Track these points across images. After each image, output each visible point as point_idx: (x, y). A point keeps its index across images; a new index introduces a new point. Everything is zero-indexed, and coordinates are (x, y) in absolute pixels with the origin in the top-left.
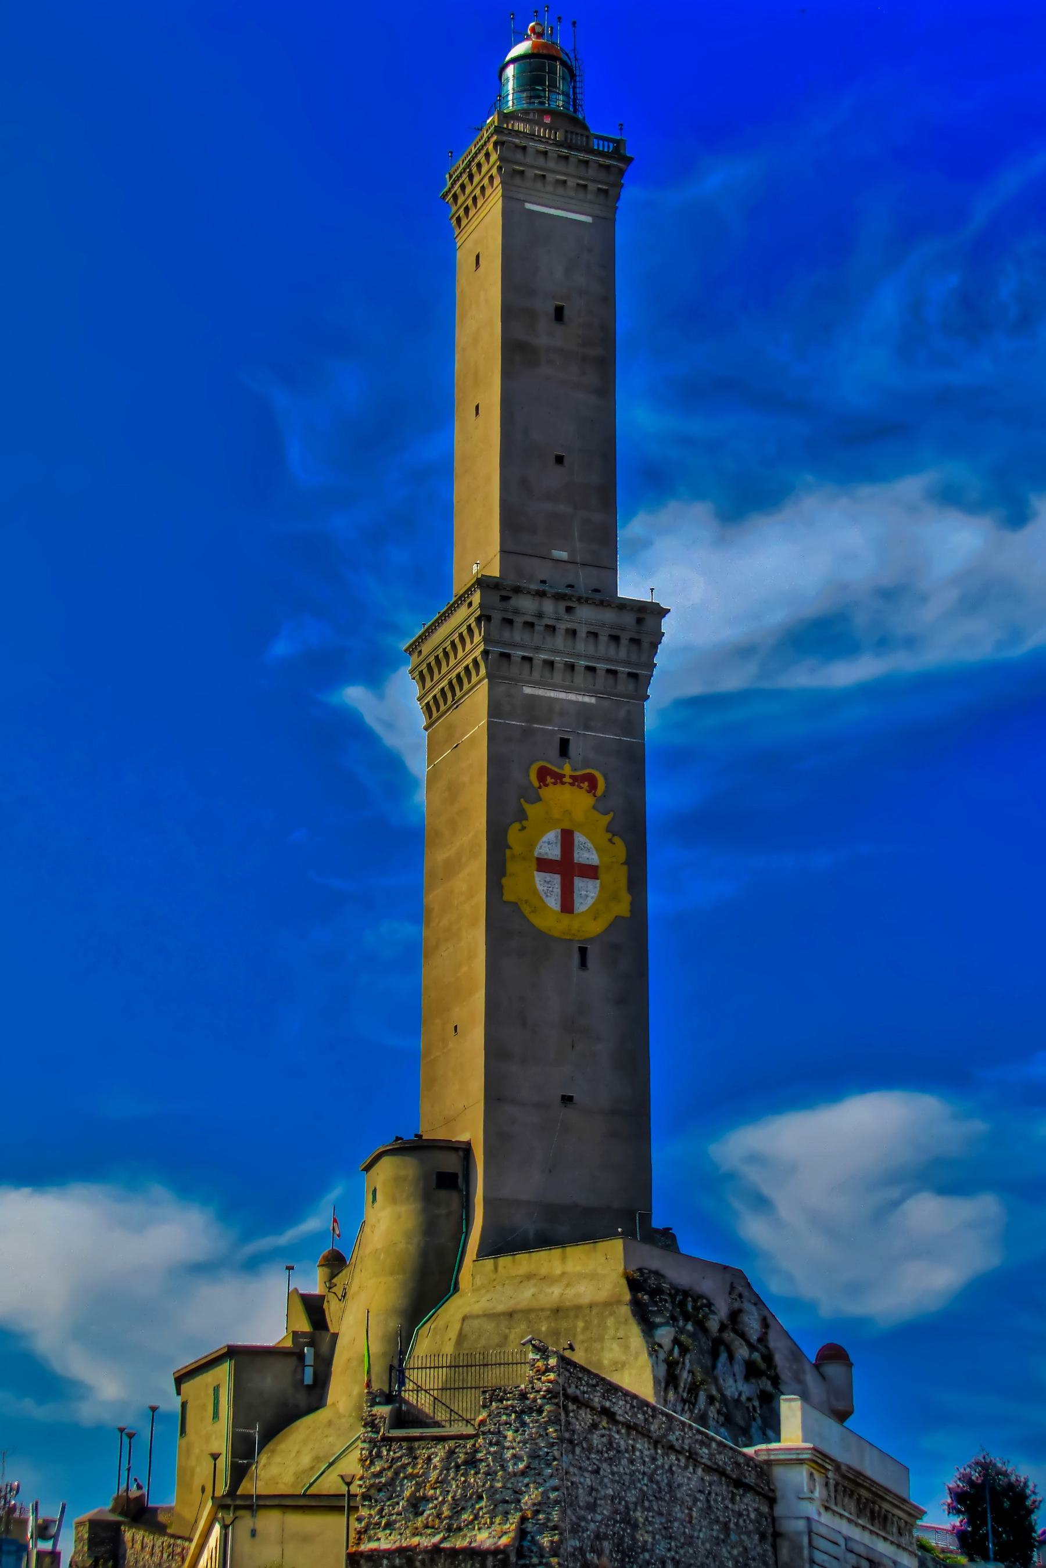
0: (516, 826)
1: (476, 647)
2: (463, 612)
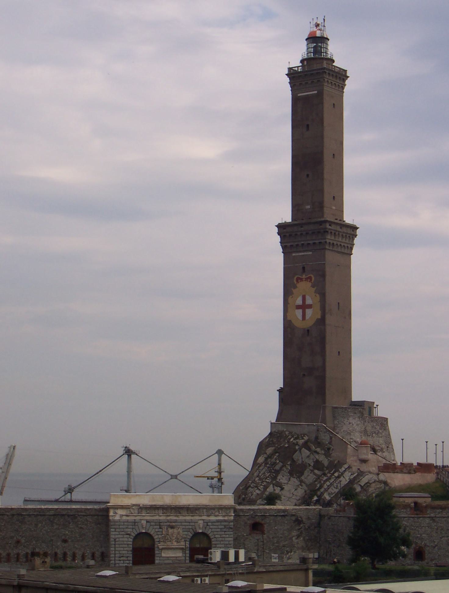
0: (291, 296)
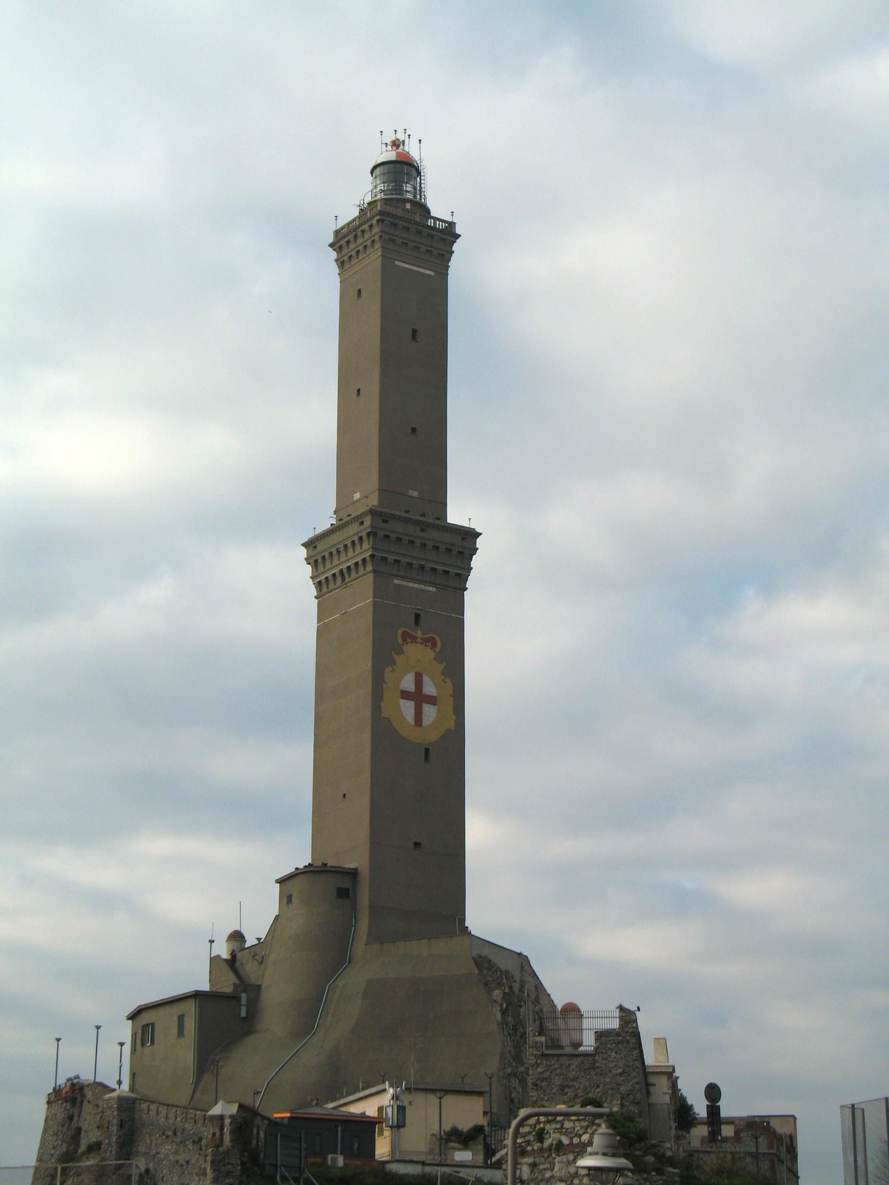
0: (389, 669)
1: (365, 550)
2: (354, 529)
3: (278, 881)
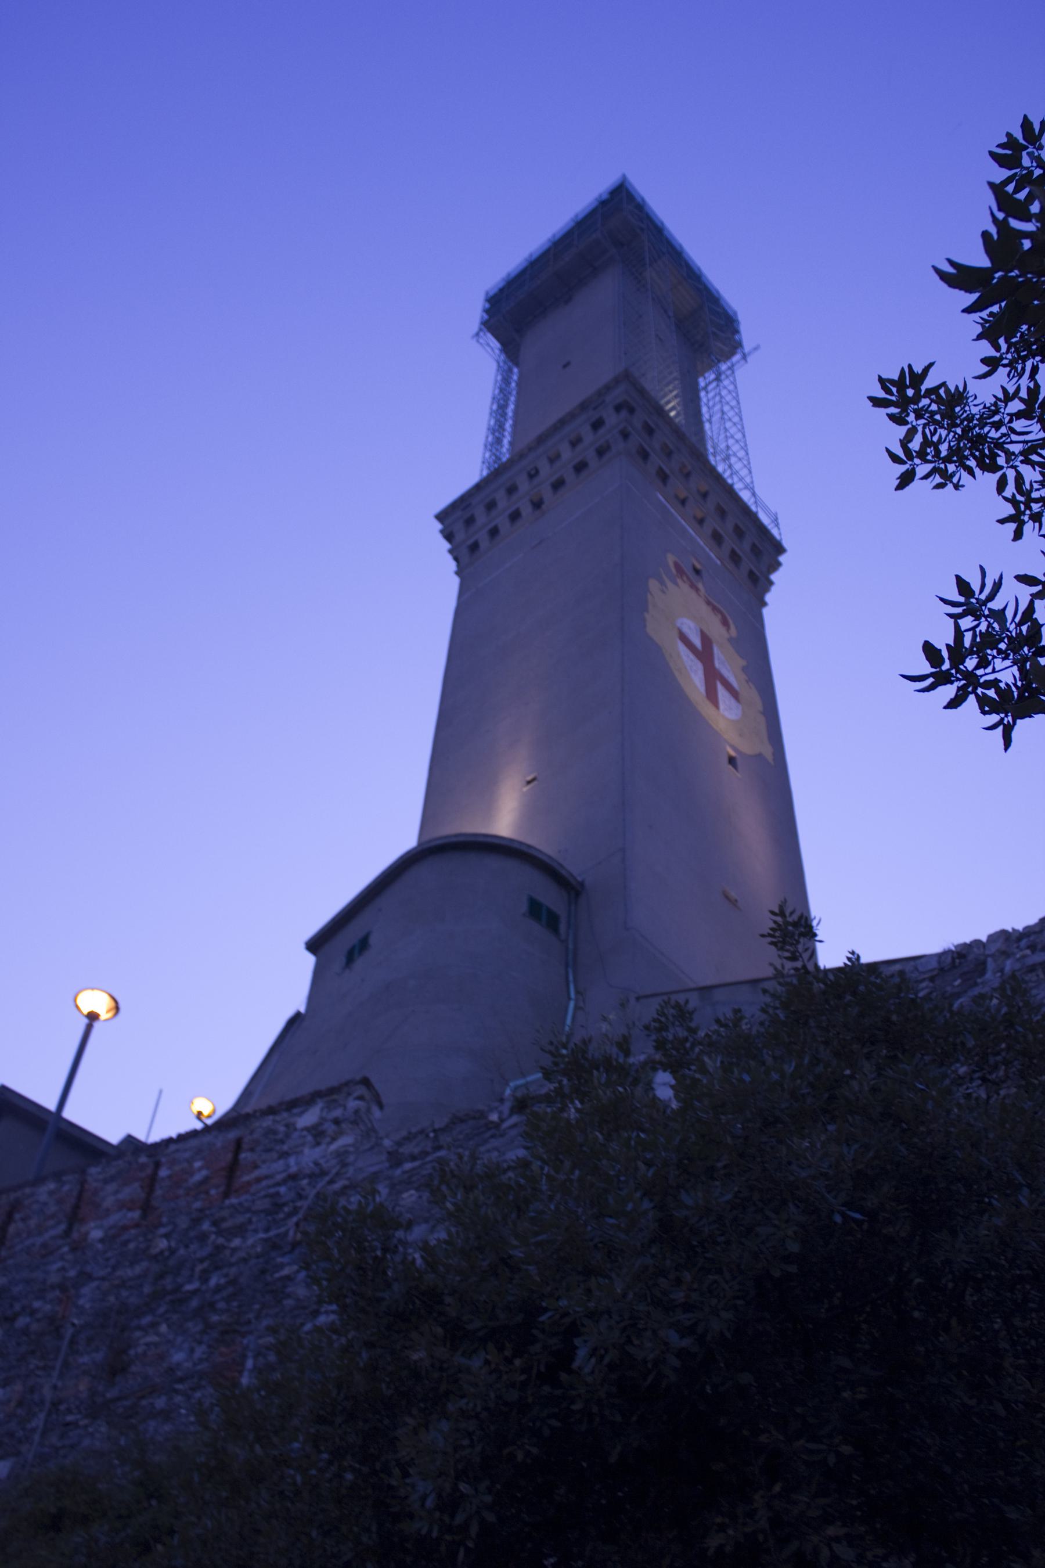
3: (314, 945)
